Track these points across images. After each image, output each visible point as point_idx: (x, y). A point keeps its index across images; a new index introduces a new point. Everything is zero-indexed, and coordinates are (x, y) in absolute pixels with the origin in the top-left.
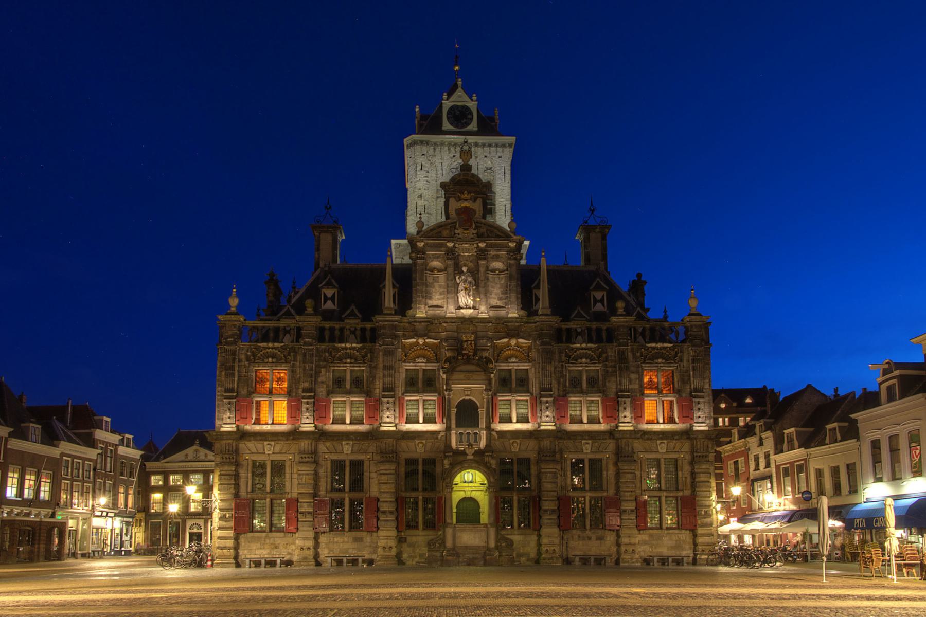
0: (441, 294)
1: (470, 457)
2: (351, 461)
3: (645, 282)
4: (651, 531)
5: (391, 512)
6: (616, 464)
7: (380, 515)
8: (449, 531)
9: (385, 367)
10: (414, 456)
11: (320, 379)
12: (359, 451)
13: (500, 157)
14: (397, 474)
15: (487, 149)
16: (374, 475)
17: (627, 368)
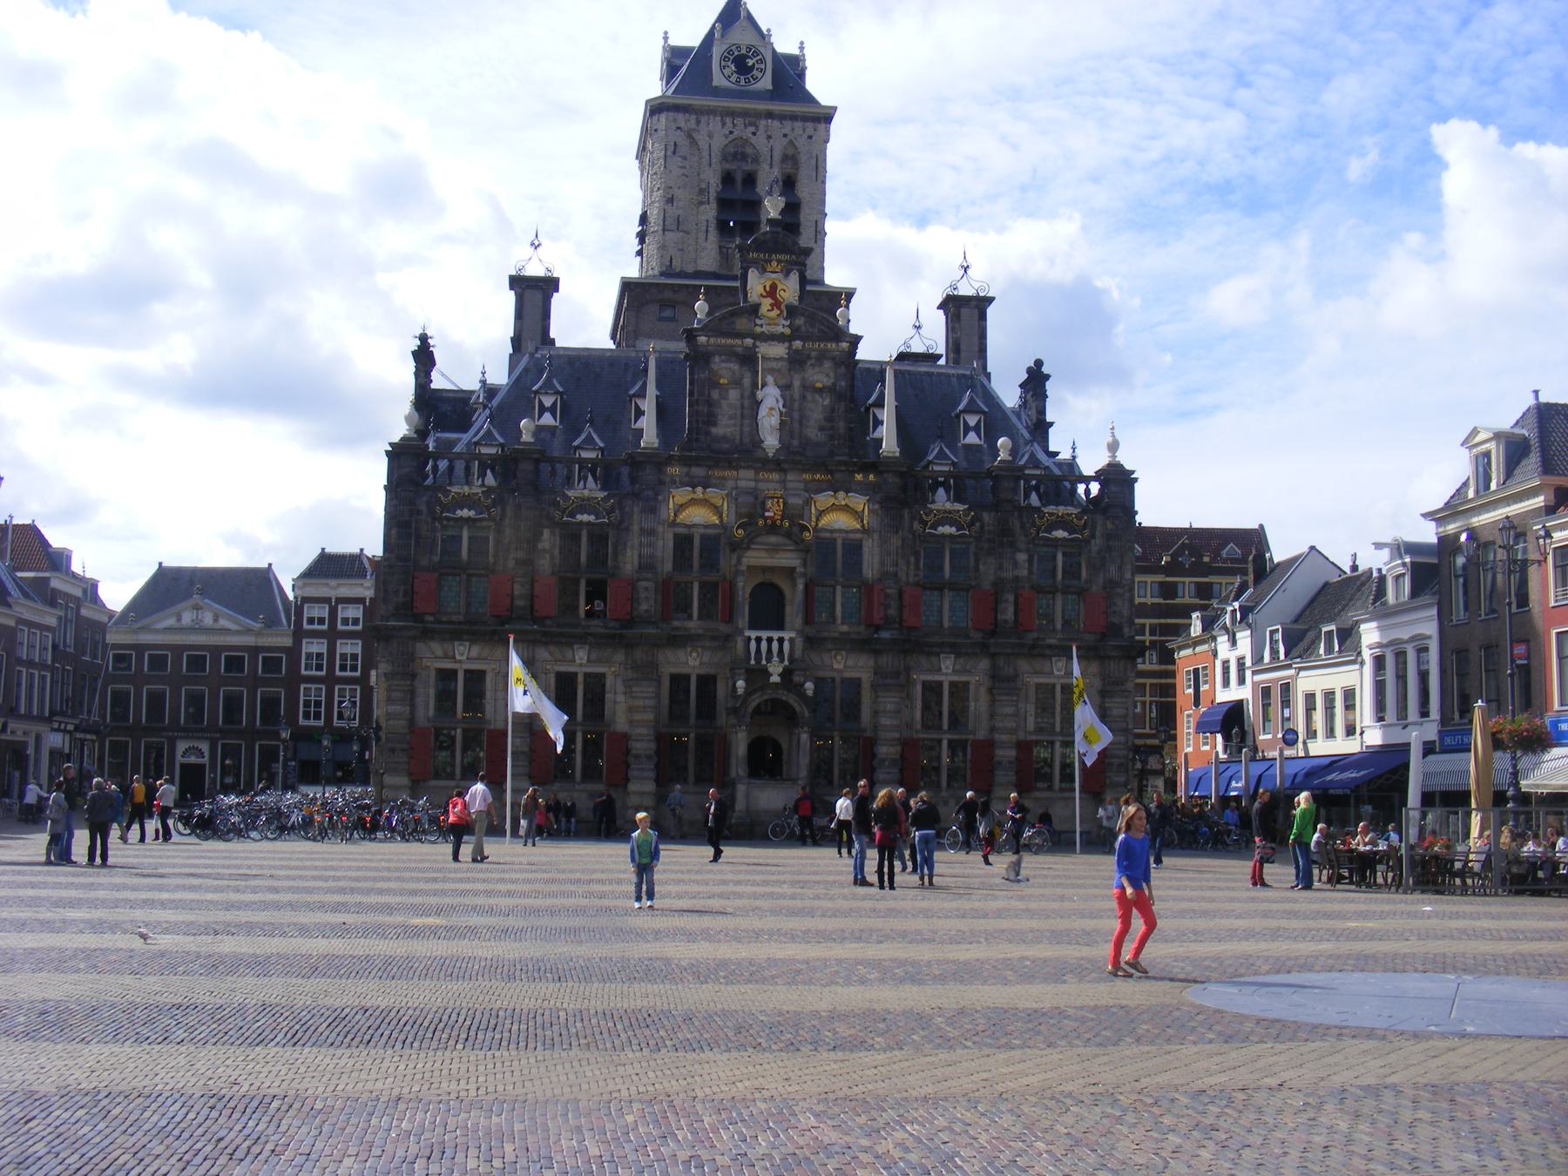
0: (731, 418)
1: (775, 679)
2: (586, 675)
3: (1047, 377)
4: (1037, 794)
5: (649, 757)
6: (990, 691)
7: (631, 759)
8: (741, 789)
9: (643, 532)
10: (684, 671)
11: (540, 546)
12: (599, 661)
13: (810, 137)
14: (658, 696)
15: (788, 125)
16: (621, 698)
17: (1012, 545)
